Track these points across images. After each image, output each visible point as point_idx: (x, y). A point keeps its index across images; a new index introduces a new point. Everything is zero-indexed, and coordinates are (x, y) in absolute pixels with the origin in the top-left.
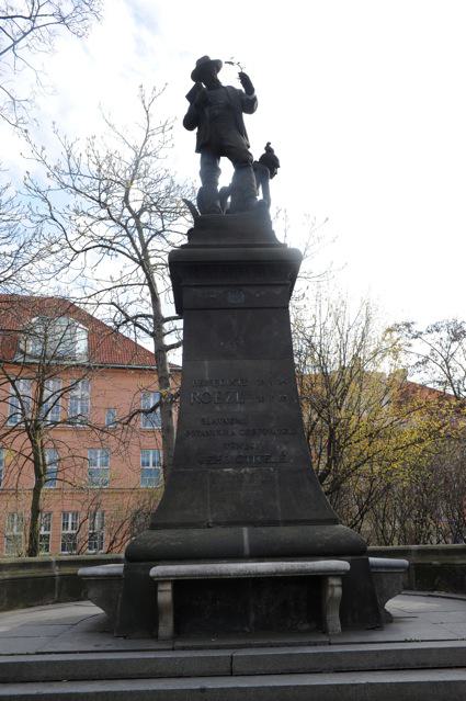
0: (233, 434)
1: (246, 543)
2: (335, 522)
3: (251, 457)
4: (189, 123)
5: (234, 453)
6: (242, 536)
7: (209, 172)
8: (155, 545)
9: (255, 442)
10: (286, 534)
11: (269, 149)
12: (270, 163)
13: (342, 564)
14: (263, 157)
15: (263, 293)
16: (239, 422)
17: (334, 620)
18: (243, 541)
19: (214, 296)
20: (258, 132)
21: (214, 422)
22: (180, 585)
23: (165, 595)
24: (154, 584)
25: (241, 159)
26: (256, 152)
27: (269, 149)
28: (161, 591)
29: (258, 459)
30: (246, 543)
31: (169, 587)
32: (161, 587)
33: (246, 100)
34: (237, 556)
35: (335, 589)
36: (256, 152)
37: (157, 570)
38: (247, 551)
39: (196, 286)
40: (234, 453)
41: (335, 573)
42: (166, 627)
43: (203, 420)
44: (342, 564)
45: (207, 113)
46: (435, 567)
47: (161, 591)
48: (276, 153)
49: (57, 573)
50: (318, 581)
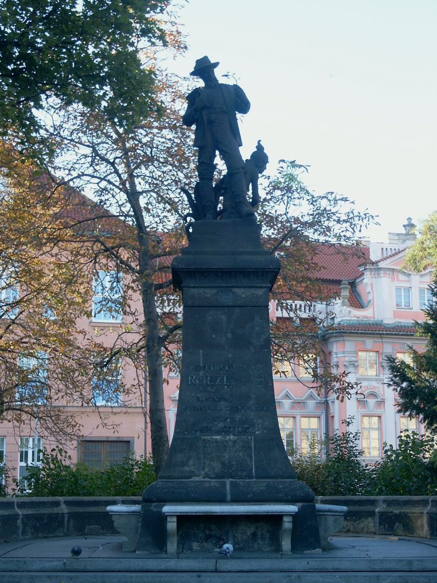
0: (221, 410)
3: (234, 428)
5: (221, 425)
7: (206, 168)
9: (238, 417)
11: (260, 148)
12: (260, 159)
13: (293, 508)
14: (254, 155)
15: (248, 293)
16: (226, 400)
17: (286, 544)
19: (208, 296)
20: (251, 131)
21: (207, 399)
22: (183, 519)
23: (172, 525)
24: (163, 518)
25: (231, 157)
26: (246, 152)
27: (260, 148)
28: (170, 522)
29: (240, 429)
31: (175, 519)
32: (169, 519)
33: (238, 101)
34: (222, 500)
35: (287, 524)
36: (246, 152)
37: (167, 509)
38: (229, 498)
39: (194, 287)
41: (288, 514)
42: (172, 546)
43: (198, 398)
45: (205, 118)
46: (396, 515)
47: (170, 522)
49: (66, 511)
50: (277, 519)
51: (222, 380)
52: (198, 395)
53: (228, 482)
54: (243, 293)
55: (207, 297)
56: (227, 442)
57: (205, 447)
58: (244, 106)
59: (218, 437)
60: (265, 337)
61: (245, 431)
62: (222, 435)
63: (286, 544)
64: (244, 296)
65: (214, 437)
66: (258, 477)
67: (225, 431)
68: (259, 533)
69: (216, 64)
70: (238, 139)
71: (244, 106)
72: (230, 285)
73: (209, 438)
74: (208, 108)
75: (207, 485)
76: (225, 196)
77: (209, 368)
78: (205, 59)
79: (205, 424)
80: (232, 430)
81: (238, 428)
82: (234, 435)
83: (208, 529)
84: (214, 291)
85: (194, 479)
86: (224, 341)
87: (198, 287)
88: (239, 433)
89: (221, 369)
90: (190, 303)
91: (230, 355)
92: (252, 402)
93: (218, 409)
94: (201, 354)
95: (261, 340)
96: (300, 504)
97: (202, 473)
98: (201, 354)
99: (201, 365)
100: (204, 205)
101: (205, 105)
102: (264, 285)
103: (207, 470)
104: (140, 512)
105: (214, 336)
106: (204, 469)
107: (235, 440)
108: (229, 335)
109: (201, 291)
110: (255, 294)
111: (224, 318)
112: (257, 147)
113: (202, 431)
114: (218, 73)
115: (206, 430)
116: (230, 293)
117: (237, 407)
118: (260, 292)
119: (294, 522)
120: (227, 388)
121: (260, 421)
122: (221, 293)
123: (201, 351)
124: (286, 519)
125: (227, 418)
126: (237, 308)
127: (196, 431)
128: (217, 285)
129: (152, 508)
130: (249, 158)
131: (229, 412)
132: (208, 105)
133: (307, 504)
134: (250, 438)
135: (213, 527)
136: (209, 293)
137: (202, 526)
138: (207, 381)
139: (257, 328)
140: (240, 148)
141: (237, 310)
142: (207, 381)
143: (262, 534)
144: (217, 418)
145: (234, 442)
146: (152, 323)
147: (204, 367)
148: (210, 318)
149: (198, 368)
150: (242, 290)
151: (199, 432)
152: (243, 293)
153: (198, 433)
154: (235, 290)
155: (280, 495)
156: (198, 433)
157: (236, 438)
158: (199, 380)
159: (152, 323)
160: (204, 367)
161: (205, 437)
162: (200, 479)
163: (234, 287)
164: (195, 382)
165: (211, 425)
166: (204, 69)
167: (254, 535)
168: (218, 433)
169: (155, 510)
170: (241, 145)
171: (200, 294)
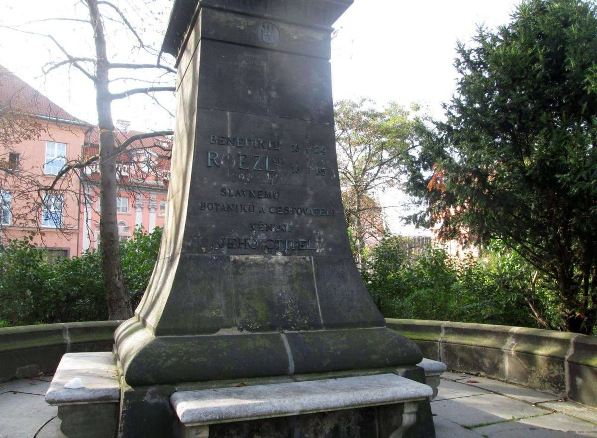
0: (262, 211)
3: (284, 242)
5: (262, 236)
9: (288, 224)
16: (268, 196)
19: (242, 28)
29: (291, 244)
40: (262, 236)
43: (223, 190)
52: (224, 185)
55: (240, 30)
56: (273, 265)
57: (236, 273)
59: (258, 258)
61: (300, 248)
64: (295, 37)
65: (252, 257)
66: (328, 326)
67: (270, 248)
68: (343, 428)
73: (243, 258)
75: (250, 344)
79: (235, 235)
80: (280, 245)
81: (289, 242)
82: (284, 254)
85: (223, 332)
87: (226, 11)
90: (212, 33)
91: (274, 125)
92: (308, 203)
93: (257, 209)
94: (229, 119)
97: (238, 321)
103: (244, 315)
105: (249, 92)
106: (239, 314)
107: (286, 263)
109: (231, 17)
113: (230, 246)
117: (286, 209)
123: (228, 114)
124: (407, 410)
129: (147, 398)
131: (273, 216)
134: (308, 259)
138: (238, 163)
142: (238, 163)
143: (349, 428)
144: (255, 224)
148: (244, 62)
151: (226, 248)
153: (224, 251)
155: (374, 357)
156: (224, 251)
157: (286, 259)
158: (225, 159)
161: (237, 257)
162: (235, 332)
164: (219, 162)
165: (246, 236)
168: (258, 249)
171: (228, 22)
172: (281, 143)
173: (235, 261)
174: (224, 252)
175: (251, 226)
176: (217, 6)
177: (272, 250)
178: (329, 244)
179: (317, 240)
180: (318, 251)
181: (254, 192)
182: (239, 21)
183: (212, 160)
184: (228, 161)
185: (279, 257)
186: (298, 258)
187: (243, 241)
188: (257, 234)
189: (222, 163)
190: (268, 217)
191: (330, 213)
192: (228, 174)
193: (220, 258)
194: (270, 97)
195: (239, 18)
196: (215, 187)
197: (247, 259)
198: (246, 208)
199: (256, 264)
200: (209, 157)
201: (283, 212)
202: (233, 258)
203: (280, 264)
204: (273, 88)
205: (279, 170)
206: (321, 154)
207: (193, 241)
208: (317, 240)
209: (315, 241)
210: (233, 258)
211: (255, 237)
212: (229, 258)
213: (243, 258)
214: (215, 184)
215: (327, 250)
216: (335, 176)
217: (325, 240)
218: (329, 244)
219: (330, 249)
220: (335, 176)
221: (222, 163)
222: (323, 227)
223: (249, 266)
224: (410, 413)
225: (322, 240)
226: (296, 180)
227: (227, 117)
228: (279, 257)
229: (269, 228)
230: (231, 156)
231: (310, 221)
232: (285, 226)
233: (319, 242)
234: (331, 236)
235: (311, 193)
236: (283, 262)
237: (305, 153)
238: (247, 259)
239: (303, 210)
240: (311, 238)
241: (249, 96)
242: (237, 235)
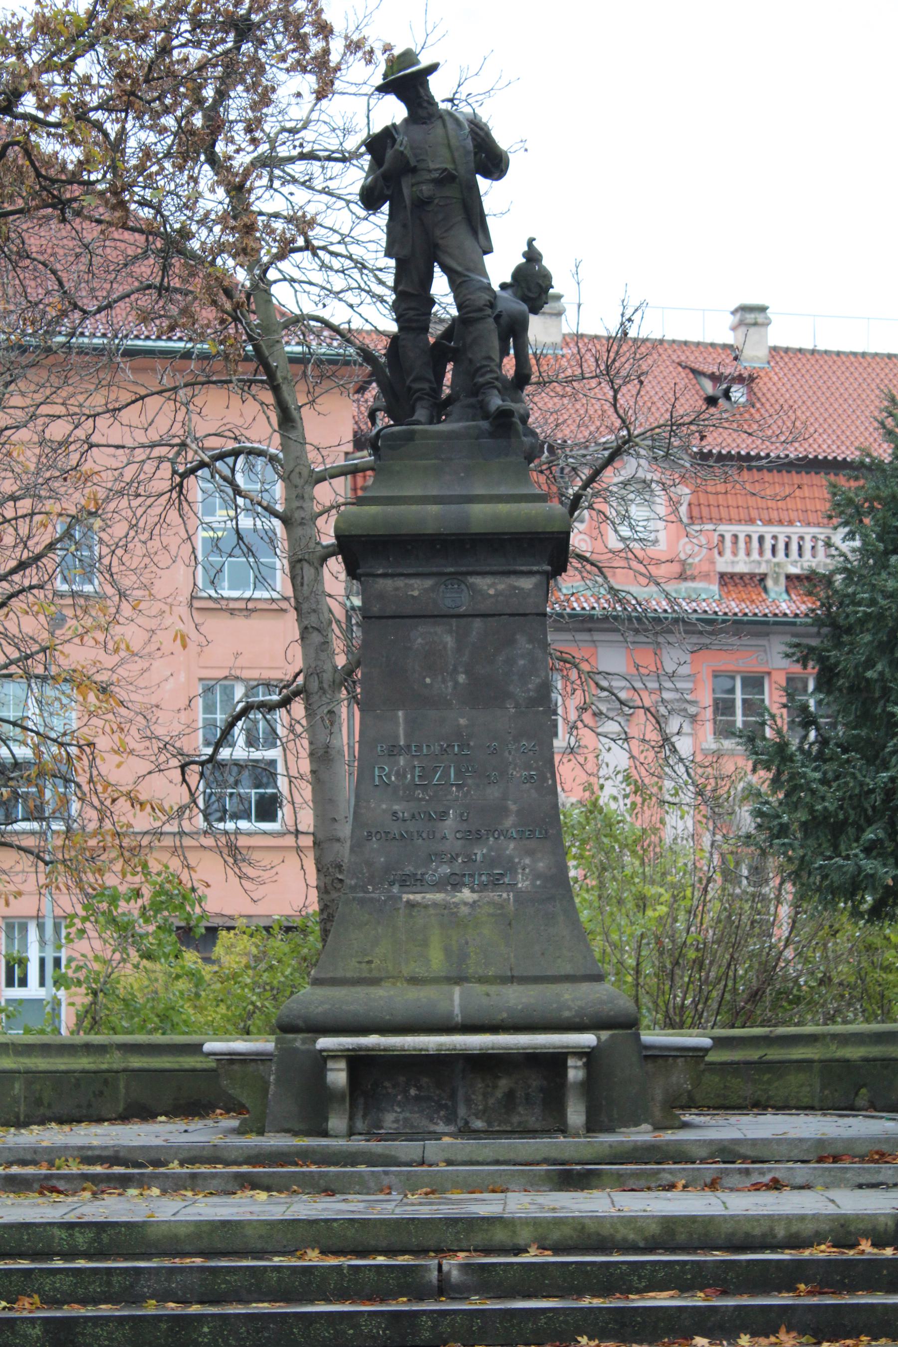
1: (457, 1010)
2: (599, 978)
4: (370, 199)
5: (446, 870)
6: (452, 1000)
7: (412, 301)
8: (320, 1009)
9: (480, 852)
10: (516, 998)
11: (532, 256)
12: (533, 285)
13: (588, 1039)
14: (519, 274)
15: (501, 587)
17: (576, 1115)
18: (453, 1006)
19: (416, 593)
20: (513, 217)
21: (413, 817)
22: (357, 1062)
26: (499, 268)
27: (532, 256)
28: (332, 1070)
29: (484, 878)
30: (457, 1010)
31: (342, 1065)
32: (330, 1065)
35: (575, 1073)
36: (499, 268)
37: (325, 1042)
39: (384, 575)
41: (580, 1053)
43: (395, 813)
44: (588, 1039)
45: (406, 191)
47: (332, 1070)
48: (547, 262)
50: (554, 1062)
51: (445, 774)
52: (396, 807)
53: (457, 991)
54: (490, 587)
55: (412, 596)
56: (456, 905)
58: (494, 163)
59: (439, 897)
60: (538, 680)
61: (495, 883)
62: (446, 891)
63: (576, 1115)
64: (492, 592)
65: (428, 896)
67: (454, 883)
68: (520, 1094)
69: (433, 68)
70: (481, 236)
71: (494, 163)
72: (464, 569)
73: (418, 897)
74: (414, 170)
76: (461, 357)
77: (419, 748)
78: (408, 57)
79: (409, 869)
83: (415, 1086)
84: (428, 583)
86: (450, 690)
87: (392, 576)
88: (483, 887)
89: (444, 751)
90: (375, 609)
91: (462, 721)
92: (509, 822)
93: (438, 835)
94: (401, 720)
95: (530, 686)
96: (605, 1035)
98: (401, 720)
99: (402, 743)
100: (410, 388)
101: (408, 163)
102: (535, 568)
104: (271, 1054)
105: (428, 680)
107: (474, 902)
108: (462, 678)
109: (400, 582)
110: (515, 588)
111: (449, 641)
112: (525, 255)
114: (439, 88)
115: (410, 881)
116: (463, 587)
118: (527, 583)
119: (588, 1066)
120: (457, 791)
121: (527, 861)
122: (443, 587)
123: (400, 713)
124: (571, 1062)
125: (458, 855)
126: (478, 620)
127: (392, 884)
128: (434, 569)
129: (298, 1044)
130: (508, 279)
131: (460, 842)
132: (413, 163)
133: (621, 1032)
135: (425, 1081)
136: (417, 587)
137: (402, 1079)
139: (521, 662)
140: (486, 258)
141: (477, 623)
145: (473, 905)
146: (316, 638)
147: (409, 747)
148: (419, 640)
149: (393, 751)
150: (489, 580)
152: (490, 586)
153: (395, 889)
154: (472, 580)
155: (567, 1014)
156: (395, 889)
157: (475, 896)
158: (397, 774)
159: (316, 638)
160: (409, 747)
161: (411, 897)
163: (471, 574)
164: (389, 778)
166: (407, 81)
167: (510, 1095)
168: (439, 886)
169: (303, 1047)
170: (488, 250)
171: (397, 589)
172: (472, 744)
173: (408, 902)
174: (395, 891)
175: (429, 859)
176: (380, 571)
177: (457, 886)
178: (538, 876)
179: (520, 871)
180: (520, 885)
181: (435, 813)
182: (412, 585)
183: (380, 776)
184: (401, 775)
185: (466, 894)
186: (493, 895)
187: (419, 877)
188: (437, 867)
189: (393, 778)
190: (453, 844)
191: (540, 833)
192: (401, 793)
193: (390, 898)
194: (456, 683)
195: (412, 581)
196: (384, 811)
197: (424, 898)
198: (424, 835)
199: (435, 905)
200: (377, 773)
201: (474, 837)
202: (405, 897)
203: (466, 904)
204: (461, 670)
205: (470, 781)
206: (531, 753)
207: (358, 878)
208: (520, 871)
209: (516, 873)
210: (405, 897)
211: (436, 871)
212: (401, 898)
213: (418, 897)
214: (384, 806)
215: (533, 884)
216: (550, 782)
217: (531, 870)
218: (538, 876)
219: (538, 883)
220: (550, 782)
221: (393, 778)
222: (531, 853)
223: (426, 907)
224: (576, 1067)
225: (527, 870)
226: (494, 793)
227: (397, 717)
228: (466, 894)
229: (453, 859)
230: (404, 770)
231: (512, 846)
232: (476, 854)
233: (523, 874)
234: (541, 864)
235: (513, 807)
236: (471, 901)
237: (506, 754)
238: (424, 898)
239: (501, 833)
240: (511, 869)
241: (426, 686)
242: (412, 869)
